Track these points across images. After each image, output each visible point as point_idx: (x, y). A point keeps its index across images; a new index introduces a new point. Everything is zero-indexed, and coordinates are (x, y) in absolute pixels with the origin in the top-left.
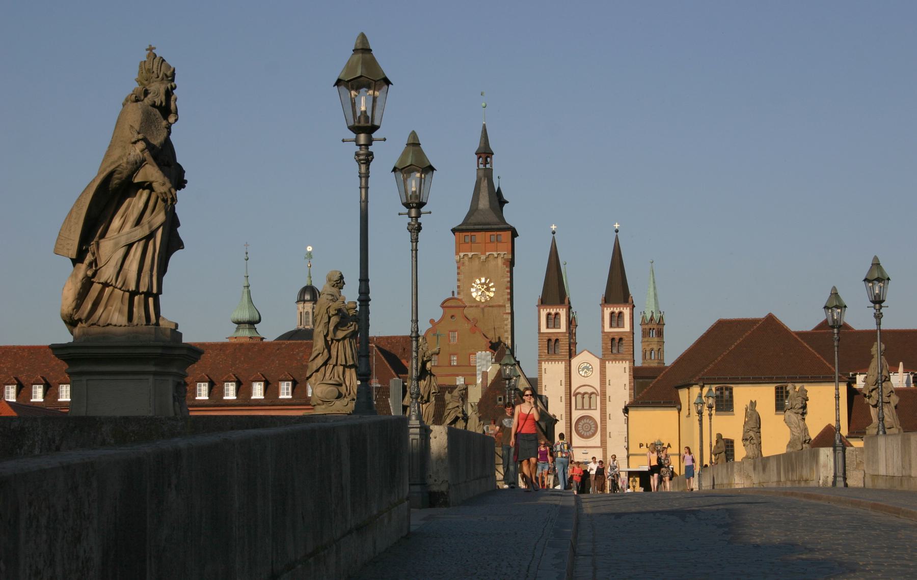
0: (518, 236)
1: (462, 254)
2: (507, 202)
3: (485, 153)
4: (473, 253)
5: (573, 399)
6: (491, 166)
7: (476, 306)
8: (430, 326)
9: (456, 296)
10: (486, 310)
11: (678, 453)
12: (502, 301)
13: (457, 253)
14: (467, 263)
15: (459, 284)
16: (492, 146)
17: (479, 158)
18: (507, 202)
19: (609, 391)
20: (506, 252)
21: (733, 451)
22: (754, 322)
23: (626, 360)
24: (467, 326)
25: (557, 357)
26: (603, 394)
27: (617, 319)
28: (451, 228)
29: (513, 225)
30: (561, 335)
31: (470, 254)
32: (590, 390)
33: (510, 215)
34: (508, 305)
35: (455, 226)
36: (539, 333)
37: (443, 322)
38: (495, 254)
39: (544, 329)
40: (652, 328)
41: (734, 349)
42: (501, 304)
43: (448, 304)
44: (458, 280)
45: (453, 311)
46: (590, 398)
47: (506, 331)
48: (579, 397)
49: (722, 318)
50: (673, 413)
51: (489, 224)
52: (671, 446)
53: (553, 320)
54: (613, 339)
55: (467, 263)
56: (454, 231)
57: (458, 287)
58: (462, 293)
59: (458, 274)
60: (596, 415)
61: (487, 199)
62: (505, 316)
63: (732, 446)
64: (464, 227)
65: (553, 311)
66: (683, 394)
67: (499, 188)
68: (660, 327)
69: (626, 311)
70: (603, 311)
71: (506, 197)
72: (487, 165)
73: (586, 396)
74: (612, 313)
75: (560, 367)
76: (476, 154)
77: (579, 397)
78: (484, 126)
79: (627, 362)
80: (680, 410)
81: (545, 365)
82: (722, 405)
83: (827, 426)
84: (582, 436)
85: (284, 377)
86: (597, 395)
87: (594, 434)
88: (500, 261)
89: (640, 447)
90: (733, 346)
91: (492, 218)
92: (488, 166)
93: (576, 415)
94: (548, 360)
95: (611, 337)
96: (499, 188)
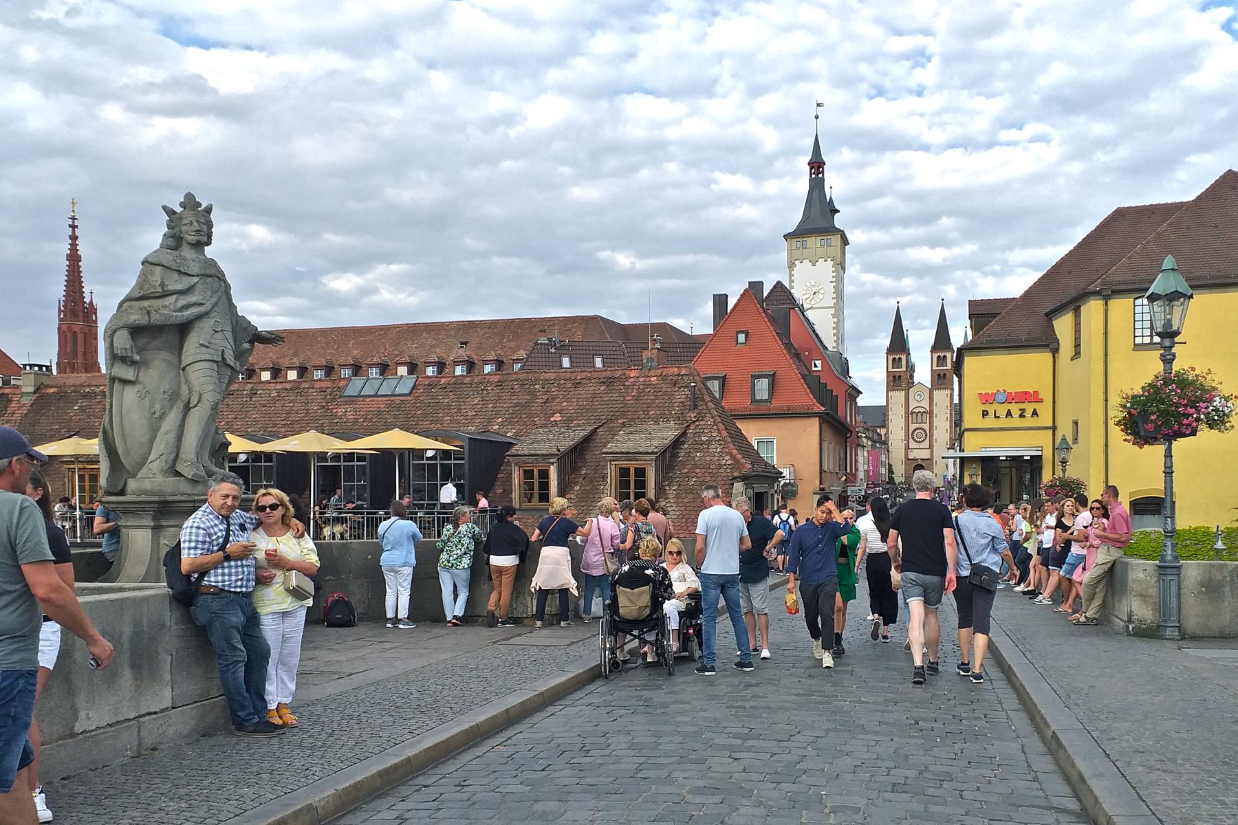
5: (910, 416)
22: (1190, 202)
23: (948, 389)
26: (931, 413)
39: (890, 370)
46: (922, 415)
48: (914, 415)
53: (897, 363)
60: (926, 427)
66: (1063, 326)
69: (949, 355)
74: (939, 357)
77: (914, 415)
80: (1055, 351)
84: (917, 441)
86: (927, 413)
87: (924, 440)
89: (983, 417)
93: (912, 427)
94: (893, 390)
95: (938, 372)
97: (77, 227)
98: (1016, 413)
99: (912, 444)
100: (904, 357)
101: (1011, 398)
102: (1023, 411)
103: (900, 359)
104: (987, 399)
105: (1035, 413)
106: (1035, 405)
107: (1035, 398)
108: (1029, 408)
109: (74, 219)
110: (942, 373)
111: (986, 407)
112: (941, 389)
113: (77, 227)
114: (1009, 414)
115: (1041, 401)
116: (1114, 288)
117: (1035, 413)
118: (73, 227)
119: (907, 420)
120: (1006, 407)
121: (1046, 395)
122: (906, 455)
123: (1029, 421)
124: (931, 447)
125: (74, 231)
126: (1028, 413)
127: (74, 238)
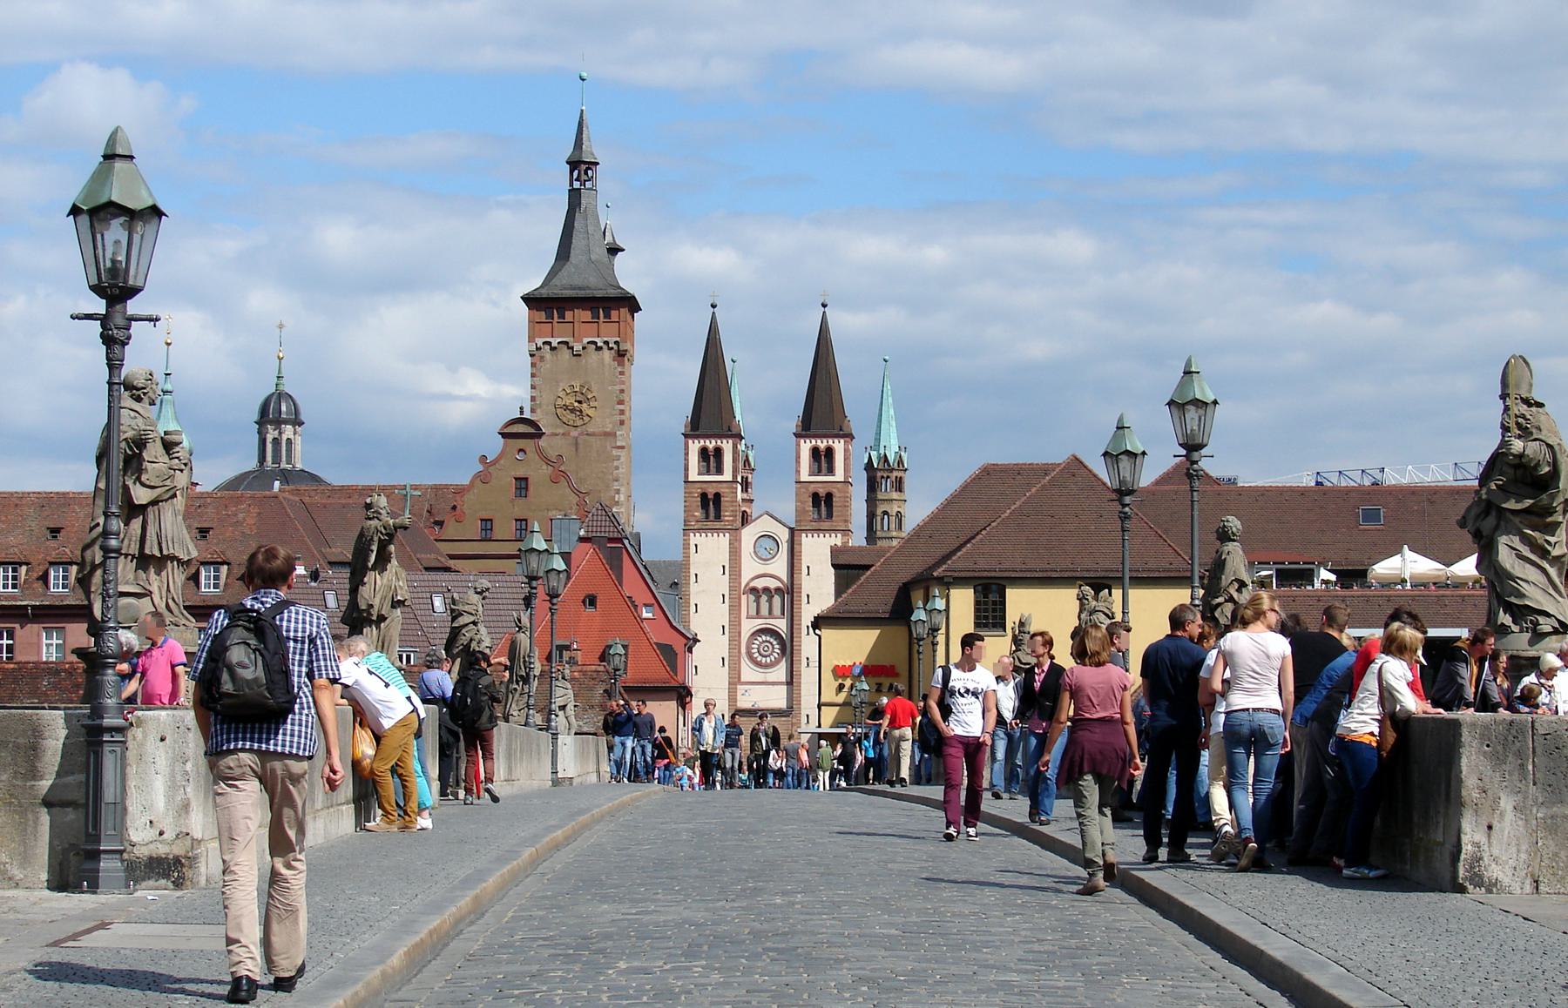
0: (641, 310)
2: (623, 250)
5: (744, 598)
7: (563, 434)
8: (480, 468)
9: (527, 415)
10: (580, 441)
12: (611, 426)
13: (531, 339)
15: (534, 395)
16: (595, 149)
18: (623, 250)
19: (806, 585)
20: (618, 339)
22: (1045, 469)
24: (546, 470)
25: (717, 525)
27: (823, 459)
28: (522, 295)
30: (724, 485)
32: (773, 584)
36: (686, 482)
37: (502, 462)
39: (694, 476)
40: (885, 476)
41: (1008, 518)
42: (608, 430)
44: (533, 387)
45: (521, 443)
51: (589, 288)
53: (711, 459)
54: (815, 496)
56: (529, 300)
57: (533, 399)
58: (538, 411)
59: (533, 375)
60: (781, 625)
65: (711, 444)
68: (899, 474)
69: (839, 446)
70: (798, 445)
71: (620, 243)
72: (587, 183)
73: (764, 598)
74: (815, 452)
75: (723, 540)
76: (567, 163)
79: (839, 535)
81: (694, 539)
82: (986, 618)
84: (759, 664)
85: (209, 556)
87: (777, 662)
88: (607, 355)
92: (588, 185)
95: (812, 488)
99: (748, 672)
100: (727, 446)
103: (718, 452)
108: (886, 682)
110: (822, 492)
112: (818, 530)
116: (956, 574)
119: (735, 609)
121: (903, 669)
122: (732, 698)
124: (791, 681)
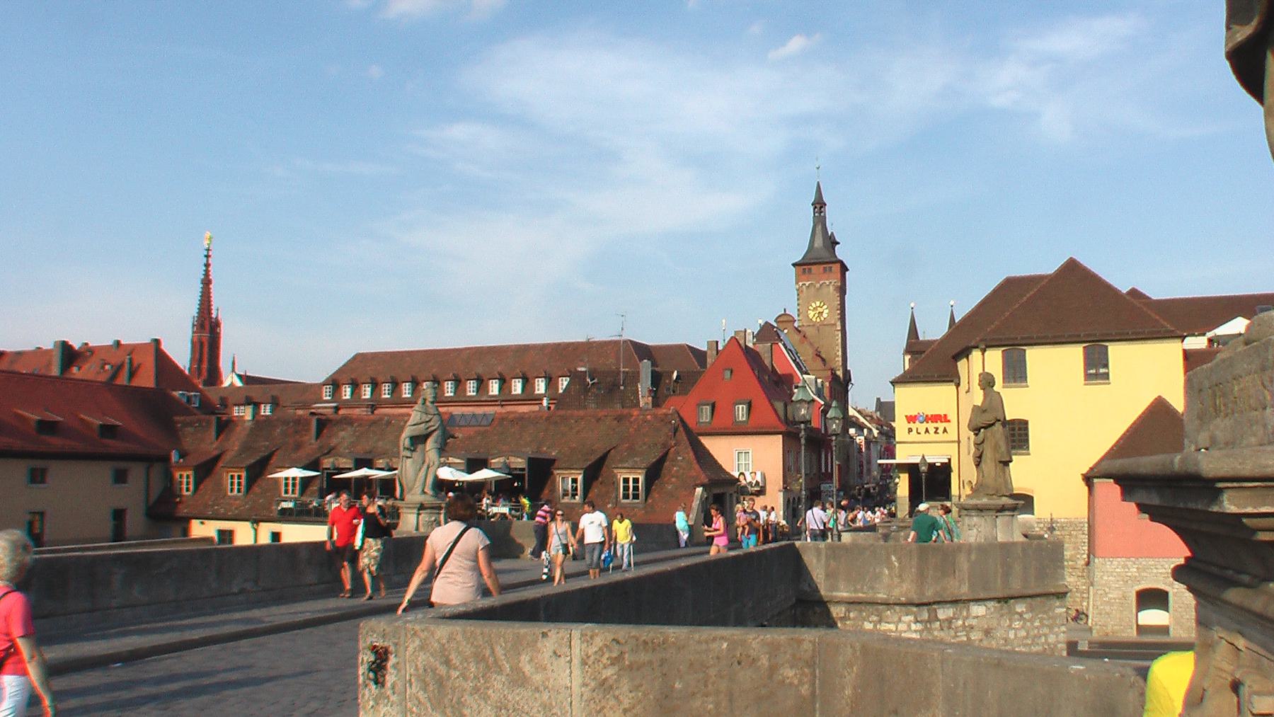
1: (801, 284)
3: (819, 205)
4: (810, 282)
6: (825, 214)
7: (814, 325)
11: (957, 439)
13: (797, 283)
14: (805, 290)
17: (814, 209)
18: (838, 243)
21: (1027, 435)
29: (841, 259)
31: (807, 284)
33: (840, 252)
34: (839, 323)
35: (794, 262)
38: (827, 282)
42: (833, 322)
43: (781, 319)
44: (798, 305)
47: (837, 345)
49: (1010, 275)
50: (951, 388)
52: (948, 430)
55: (805, 290)
56: (794, 265)
57: (798, 310)
58: (801, 315)
59: (798, 299)
61: (821, 239)
62: (836, 333)
63: (1026, 429)
64: (802, 262)
67: (832, 233)
71: (838, 240)
76: (812, 205)
78: (818, 183)
80: (958, 385)
83: (1156, 399)
88: (831, 288)
89: (909, 433)
90: (1025, 298)
91: (825, 255)
92: (822, 214)
96: (832, 233)
97: (210, 256)
98: (932, 431)
101: (928, 419)
102: (937, 429)
104: (911, 419)
105: (945, 431)
106: (945, 424)
107: (944, 419)
108: (941, 426)
109: (208, 250)
111: (912, 425)
113: (210, 256)
114: (927, 431)
115: (949, 421)
117: (945, 431)
118: (208, 256)
120: (925, 425)
123: (941, 436)
125: (207, 261)
126: (941, 431)
127: (207, 265)
